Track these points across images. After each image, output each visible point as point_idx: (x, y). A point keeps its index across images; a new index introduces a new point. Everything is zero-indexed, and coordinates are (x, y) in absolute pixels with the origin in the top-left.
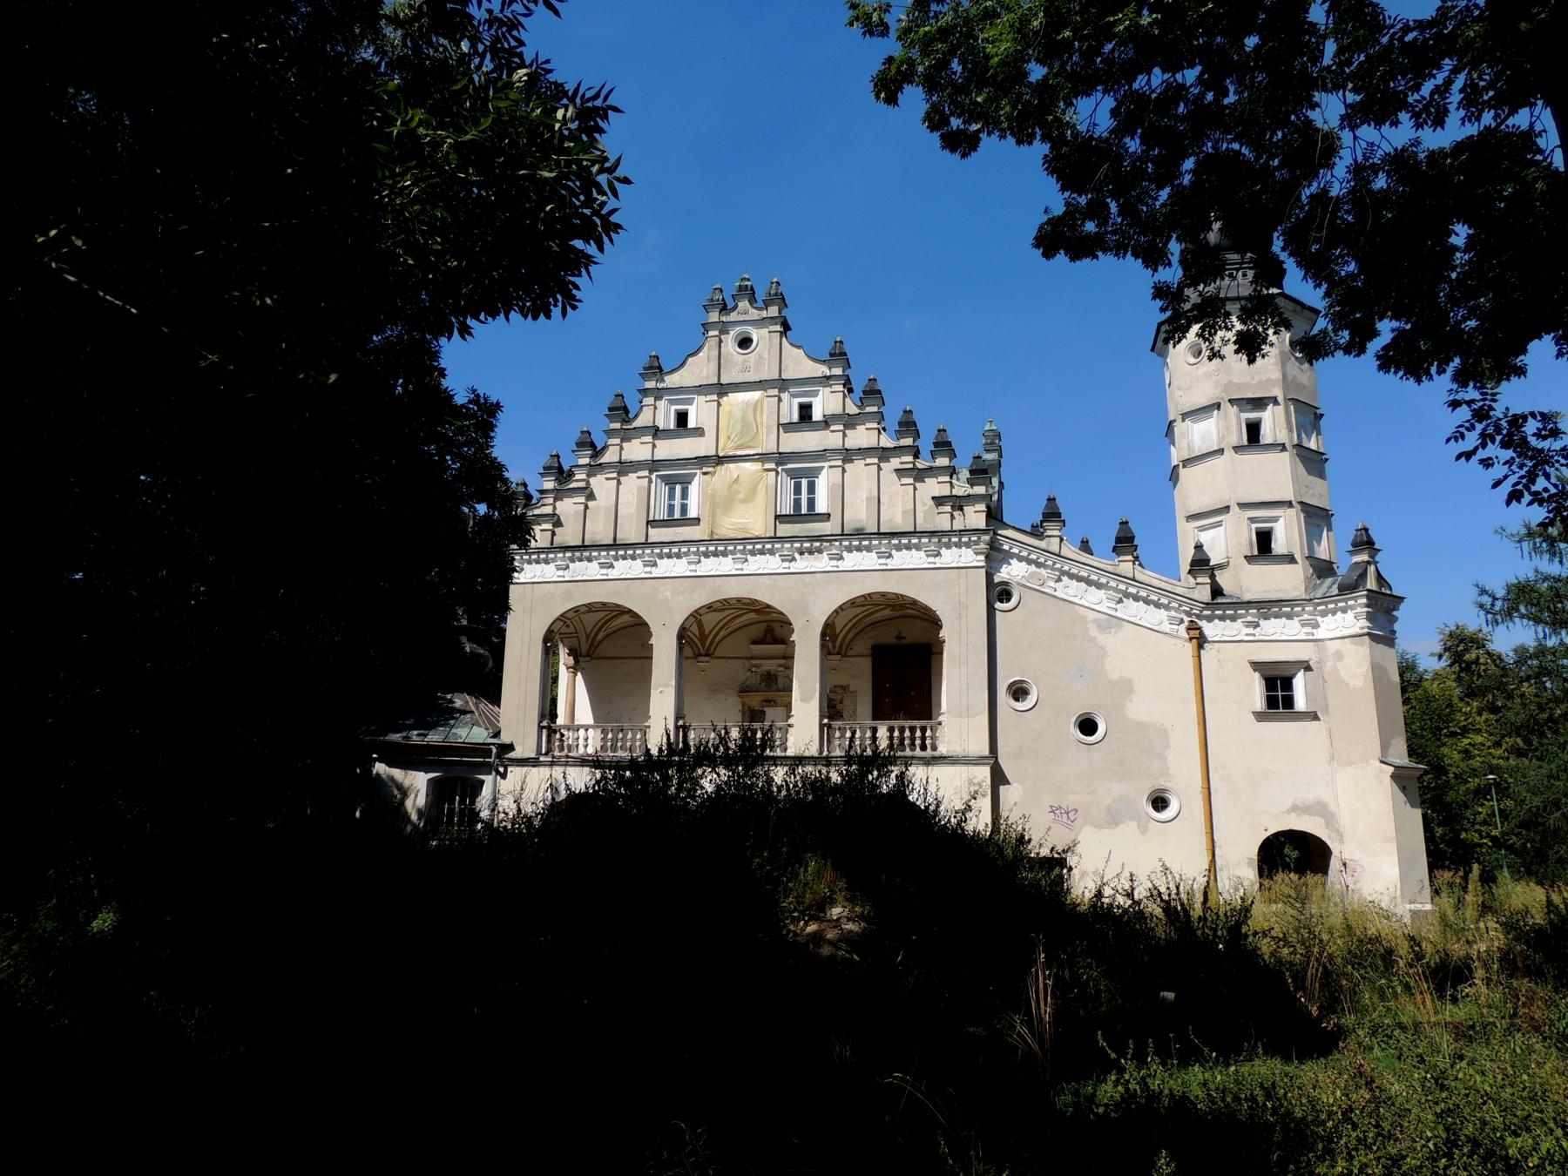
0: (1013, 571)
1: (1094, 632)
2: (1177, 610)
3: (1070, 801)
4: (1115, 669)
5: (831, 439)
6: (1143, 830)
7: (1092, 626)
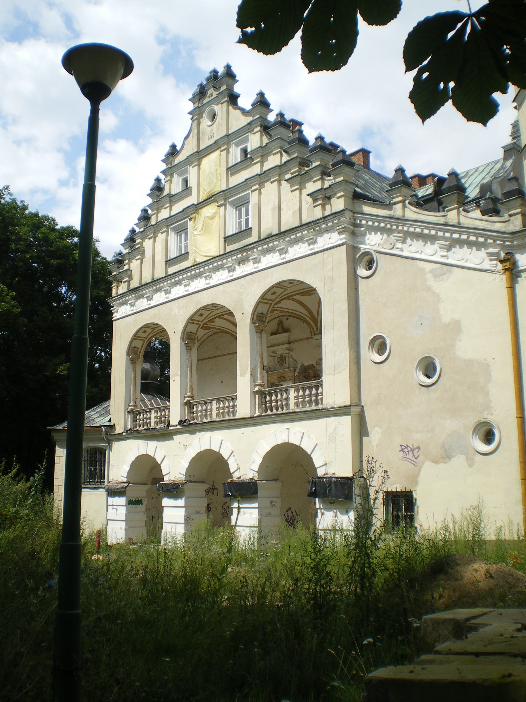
0: (373, 242)
1: (431, 281)
2: (494, 245)
3: (416, 439)
4: (447, 313)
5: (256, 169)
6: (470, 463)
7: (429, 276)
